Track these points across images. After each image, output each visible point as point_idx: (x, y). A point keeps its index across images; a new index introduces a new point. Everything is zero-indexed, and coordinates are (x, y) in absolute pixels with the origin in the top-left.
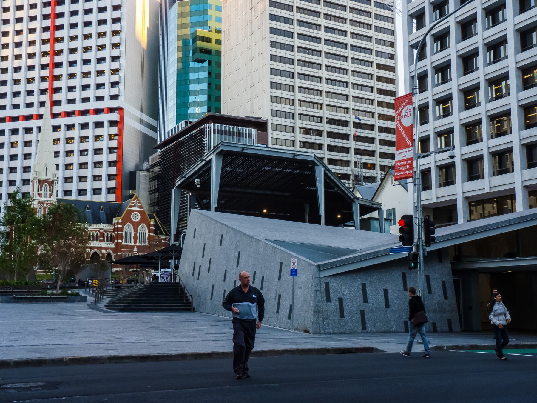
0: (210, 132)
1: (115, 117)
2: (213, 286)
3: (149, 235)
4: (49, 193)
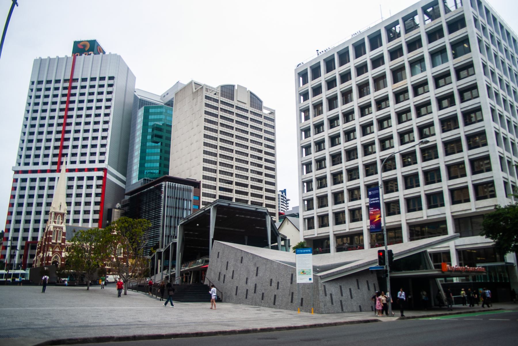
0: (165, 187)
1: (101, 174)
2: (237, 287)
4: (61, 221)
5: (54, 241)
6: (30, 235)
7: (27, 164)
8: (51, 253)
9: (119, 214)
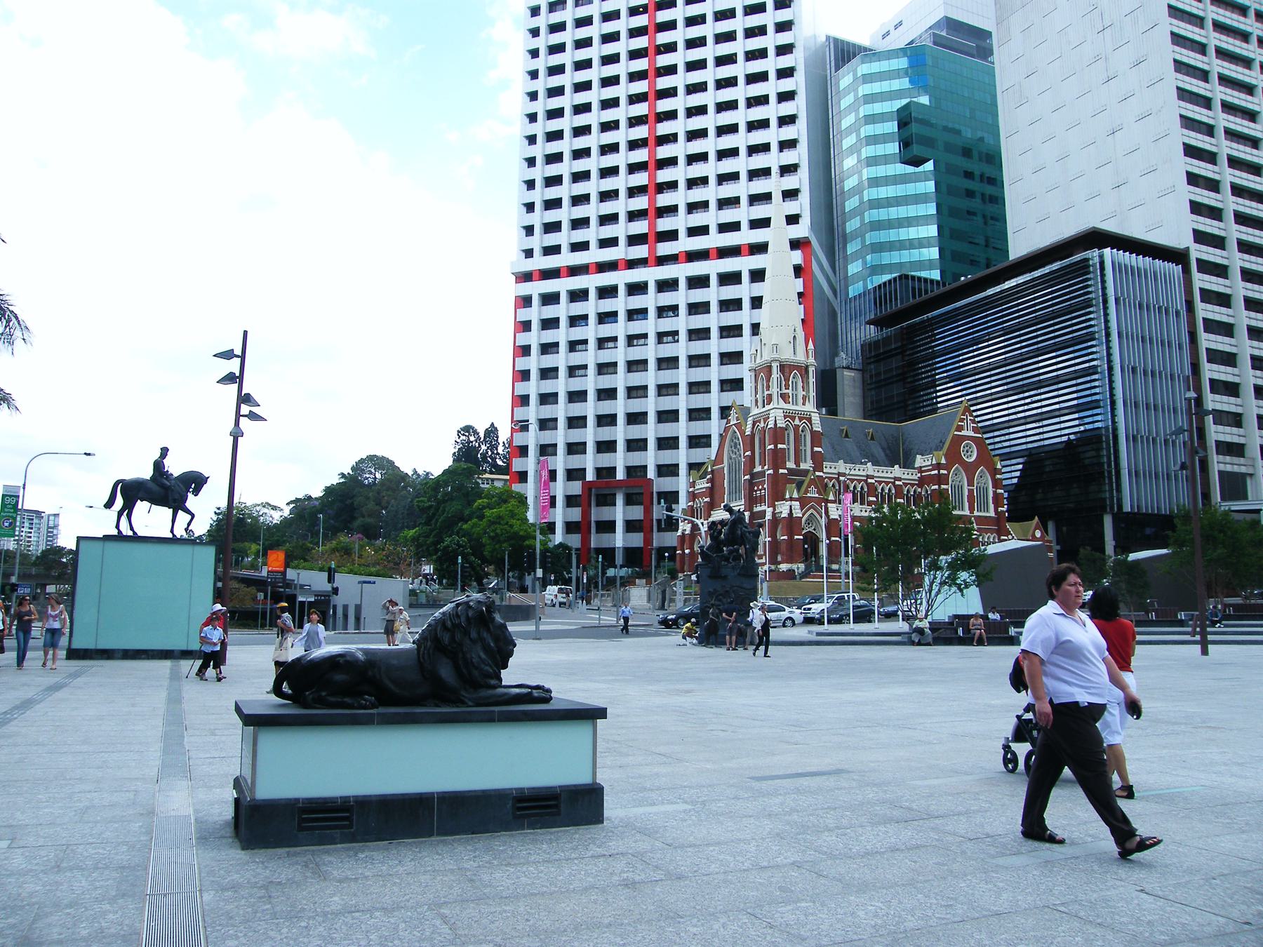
3: (995, 493)
4: (801, 393)
5: (791, 465)
6: (590, 462)
7: (553, 250)
8: (796, 504)
9: (859, 384)
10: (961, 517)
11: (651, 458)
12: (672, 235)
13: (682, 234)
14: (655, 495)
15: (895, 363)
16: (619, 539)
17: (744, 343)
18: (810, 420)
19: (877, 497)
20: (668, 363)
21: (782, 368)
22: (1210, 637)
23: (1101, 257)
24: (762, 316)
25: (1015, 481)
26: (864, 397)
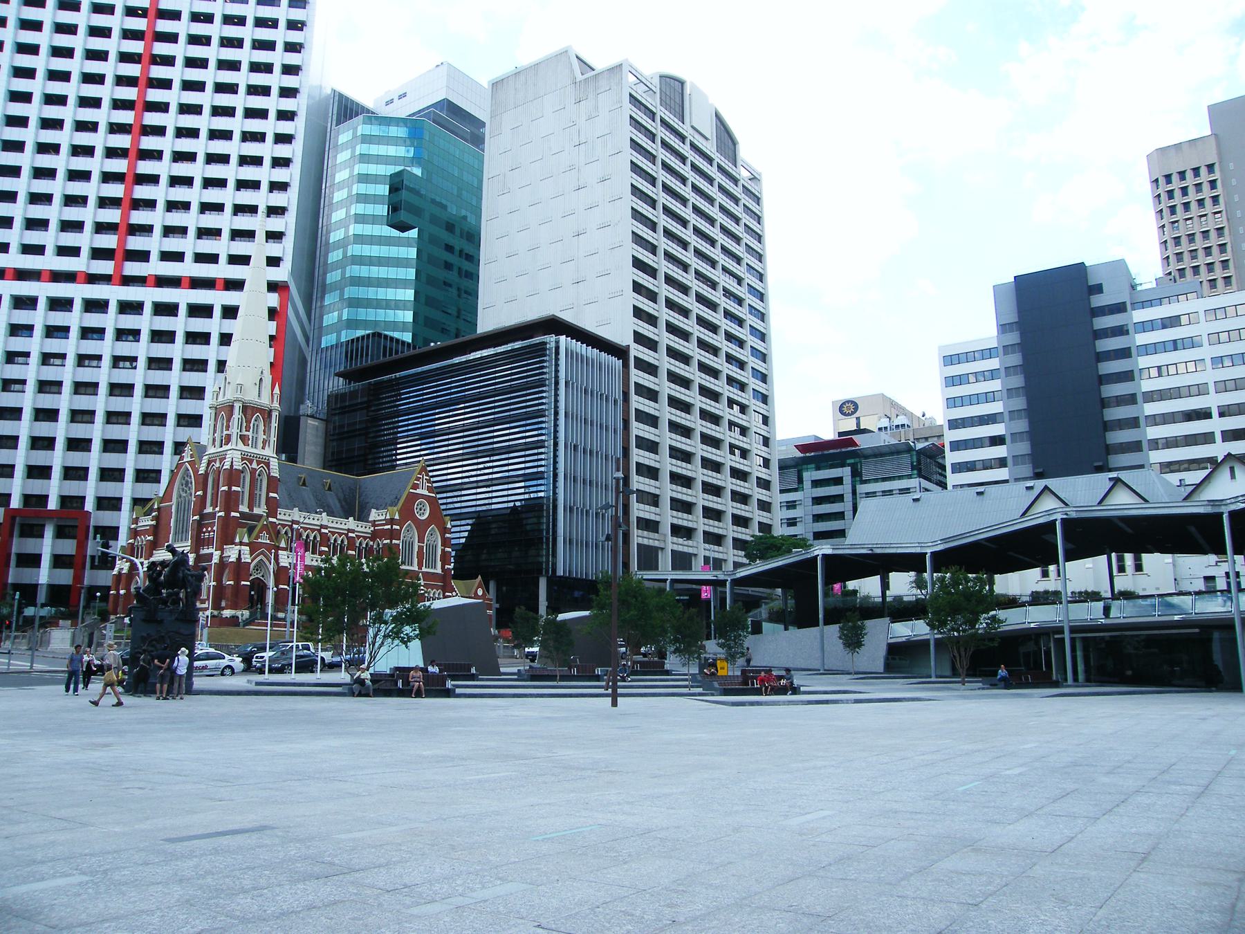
3: (443, 551)
4: (262, 437)
5: (244, 508)
9: (321, 433)
10: (407, 572)
11: (91, 489)
12: (143, 256)
13: (154, 256)
14: (91, 530)
15: (360, 417)
16: (44, 575)
17: (207, 379)
18: (268, 465)
19: (329, 547)
20: (123, 390)
21: (246, 409)
22: (620, 691)
23: (557, 342)
24: (230, 354)
25: (463, 541)
26: (326, 447)
